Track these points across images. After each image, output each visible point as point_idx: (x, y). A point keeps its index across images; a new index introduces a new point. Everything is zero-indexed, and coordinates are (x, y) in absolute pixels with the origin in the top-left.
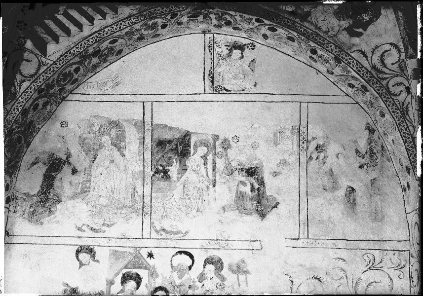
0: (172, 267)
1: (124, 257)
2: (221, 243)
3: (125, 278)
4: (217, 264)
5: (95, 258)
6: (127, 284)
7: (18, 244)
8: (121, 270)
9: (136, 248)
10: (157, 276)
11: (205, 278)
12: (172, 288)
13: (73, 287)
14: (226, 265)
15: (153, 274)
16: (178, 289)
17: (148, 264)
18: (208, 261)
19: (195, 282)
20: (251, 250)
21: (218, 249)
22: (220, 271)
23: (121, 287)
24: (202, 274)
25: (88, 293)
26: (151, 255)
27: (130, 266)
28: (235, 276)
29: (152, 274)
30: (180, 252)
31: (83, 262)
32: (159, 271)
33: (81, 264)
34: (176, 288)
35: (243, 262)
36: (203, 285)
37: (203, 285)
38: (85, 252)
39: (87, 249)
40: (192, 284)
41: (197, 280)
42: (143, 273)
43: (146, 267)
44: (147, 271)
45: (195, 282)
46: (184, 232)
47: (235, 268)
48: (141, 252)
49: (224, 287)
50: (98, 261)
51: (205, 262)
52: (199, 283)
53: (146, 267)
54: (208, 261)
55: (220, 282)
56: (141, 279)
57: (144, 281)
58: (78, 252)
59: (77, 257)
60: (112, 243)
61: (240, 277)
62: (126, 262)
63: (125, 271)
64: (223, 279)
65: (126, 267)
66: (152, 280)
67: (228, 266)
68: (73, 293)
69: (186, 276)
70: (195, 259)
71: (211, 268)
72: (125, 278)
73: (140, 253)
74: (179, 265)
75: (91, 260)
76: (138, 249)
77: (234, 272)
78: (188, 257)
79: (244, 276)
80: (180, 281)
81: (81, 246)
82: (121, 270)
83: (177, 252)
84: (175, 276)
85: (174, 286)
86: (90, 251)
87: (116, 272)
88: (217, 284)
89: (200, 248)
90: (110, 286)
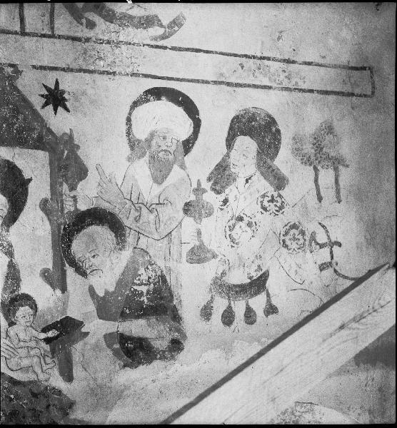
0: (133, 144)
2: (272, 70)
10: (82, 173)
11: (231, 179)
12: (134, 214)
15: (68, 165)
16: (152, 217)
19: (204, 191)
22: (273, 158)
29: (66, 167)
30: (157, 93)
32: (90, 155)
34: (144, 211)
36: (225, 201)
37: (225, 201)
40: (193, 198)
41: (207, 185)
42: (34, 165)
44: (42, 156)
45: (204, 191)
46: (165, 22)
47: (309, 149)
49: (281, 208)
51: (231, 128)
53: (40, 138)
55: (271, 190)
56: (24, 183)
57: (39, 190)
61: (322, 173)
66: (65, 187)
69: (176, 173)
70: (202, 116)
71: (246, 144)
73: (16, 89)
74: (152, 135)
77: (307, 161)
78: (179, 111)
80: (157, 189)
85: (138, 205)
88: (264, 196)
89: (215, 82)
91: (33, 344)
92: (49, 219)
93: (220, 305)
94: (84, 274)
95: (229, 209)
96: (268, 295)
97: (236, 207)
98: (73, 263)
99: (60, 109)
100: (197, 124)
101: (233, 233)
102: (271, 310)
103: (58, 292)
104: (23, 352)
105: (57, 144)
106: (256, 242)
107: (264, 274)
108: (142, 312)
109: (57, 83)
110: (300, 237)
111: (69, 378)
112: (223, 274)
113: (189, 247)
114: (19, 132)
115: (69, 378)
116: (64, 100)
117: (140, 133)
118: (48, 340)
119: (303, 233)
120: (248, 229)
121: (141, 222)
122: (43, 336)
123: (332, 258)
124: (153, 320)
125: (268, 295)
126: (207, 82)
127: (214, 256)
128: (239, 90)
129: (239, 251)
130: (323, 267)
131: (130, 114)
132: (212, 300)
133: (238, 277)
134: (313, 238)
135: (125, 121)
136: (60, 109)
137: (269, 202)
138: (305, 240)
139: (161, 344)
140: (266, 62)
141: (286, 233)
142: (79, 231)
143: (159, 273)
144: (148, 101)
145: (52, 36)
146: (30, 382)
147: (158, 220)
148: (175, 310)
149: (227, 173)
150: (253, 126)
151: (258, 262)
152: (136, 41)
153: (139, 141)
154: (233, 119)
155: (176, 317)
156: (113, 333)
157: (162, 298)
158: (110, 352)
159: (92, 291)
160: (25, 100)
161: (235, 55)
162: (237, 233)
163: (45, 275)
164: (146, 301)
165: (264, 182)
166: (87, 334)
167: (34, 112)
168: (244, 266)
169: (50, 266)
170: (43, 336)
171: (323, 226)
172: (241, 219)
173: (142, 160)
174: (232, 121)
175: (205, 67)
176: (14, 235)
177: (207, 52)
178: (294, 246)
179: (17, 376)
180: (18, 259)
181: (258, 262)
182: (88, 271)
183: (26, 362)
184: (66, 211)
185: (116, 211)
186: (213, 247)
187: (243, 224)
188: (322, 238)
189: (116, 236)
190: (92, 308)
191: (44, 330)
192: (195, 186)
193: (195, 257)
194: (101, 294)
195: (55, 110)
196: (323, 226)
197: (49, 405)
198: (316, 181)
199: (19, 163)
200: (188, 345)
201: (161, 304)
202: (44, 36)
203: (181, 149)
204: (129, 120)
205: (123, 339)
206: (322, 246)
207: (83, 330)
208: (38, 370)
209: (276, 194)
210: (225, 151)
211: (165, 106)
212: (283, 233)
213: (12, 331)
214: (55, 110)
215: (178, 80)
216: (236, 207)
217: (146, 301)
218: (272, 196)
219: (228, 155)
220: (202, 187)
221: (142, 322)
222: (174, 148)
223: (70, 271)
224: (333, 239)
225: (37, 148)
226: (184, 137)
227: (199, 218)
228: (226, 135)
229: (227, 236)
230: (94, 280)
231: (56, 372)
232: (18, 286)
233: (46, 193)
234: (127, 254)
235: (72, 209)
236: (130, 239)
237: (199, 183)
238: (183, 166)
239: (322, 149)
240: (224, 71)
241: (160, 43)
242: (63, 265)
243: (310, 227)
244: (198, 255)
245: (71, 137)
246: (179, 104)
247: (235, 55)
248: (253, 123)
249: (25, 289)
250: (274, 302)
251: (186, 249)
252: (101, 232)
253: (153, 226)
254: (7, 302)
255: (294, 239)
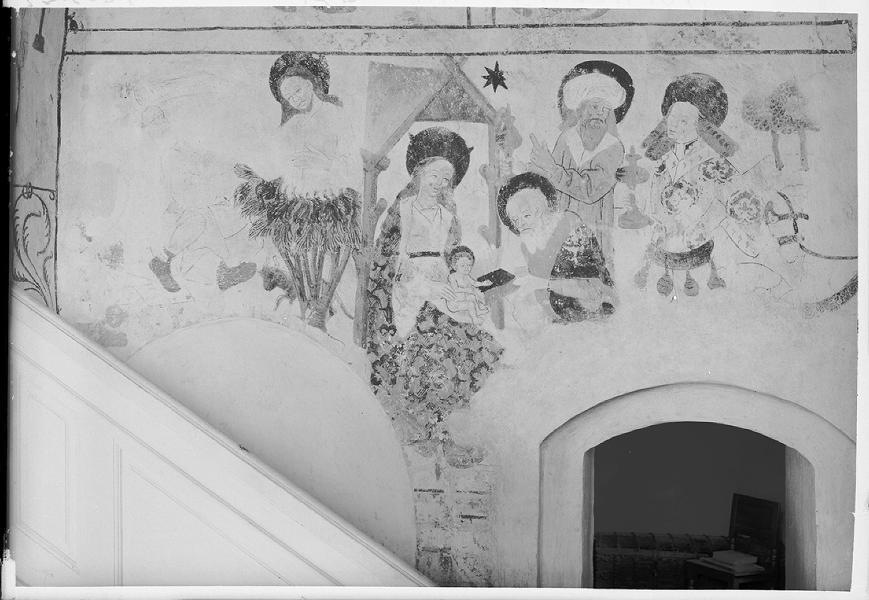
0: (564, 113)
1: (415, 84)
2: (718, 35)
3: (421, 150)
4: (711, 101)
5: (326, 91)
6: (427, 168)
7: (104, 53)
8: (406, 126)
9: (450, 56)
10: (518, 142)
12: (566, 178)
13: (267, 180)
14: (734, 103)
16: (584, 181)
17: (491, 107)
18: (677, 93)
20: (818, 52)
21: (709, 52)
22: (717, 124)
23: (408, 178)
24: (658, 134)
25: (312, 197)
26: (496, 78)
27: (433, 112)
28: (766, 137)
29: (502, 137)
31: (293, 104)
32: (524, 125)
33: (288, 111)
34: (576, 176)
35: (793, 90)
36: (662, 168)
37: (662, 168)
38: (298, 74)
39: (302, 63)
40: (626, 164)
41: (641, 152)
42: (474, 134)
43: (481, 114)
44: (483, 127)
47: (765, 112)
48: (465, 68)
50: (335, 100)
52: (648, 160)
53: (481, 114)
54: (677, 93)
55: (716, 157)
57: (478, 159)
58: (276, 74)
59: (275, 88)
60: (378, 44)
61: (783, 138)
62: (420, 102)
63: (417, 128)
64: (726, 147)
65: (421, 117)
66: (502, 155)
67: (741, 105)
68: (268, 198)
69: (608, 141)
70: (635, 85)
71: (685, 110)
72: (421, 150)
74: (583, 106)
75: (316, 98)
76: (457, 58)
78: (612, 81)
79: (795, 137)
81: (286, 56)
82: (406, 126)
83: (578, 67)
84: (574, 139)
85: (570, 170)
86: (313, 69)
87: (391, 131)
88: (707, 162)
89: (651, 52)
90: (376, 176)
91: (470, 291)
92: (488, 183)
93: (657, 271)
94: (517, 232)
95: (666, 176)
96: (713, 268)
97: (675, 172)
98: (508, 222)
99: (499, 87)
100: (630, 93)
101: (670, 200)
102: (717, 283)
103: (493, 247)
104: (460, 297)
105: (495, 116)
106: (697, 210)
107: (708, 243)
108: (574, 272)
109: (497, 65)
110: (753, 206)
111: (501, 326)
112: (660, 240)
113: (623, 212)
114: (464, 108)
115: (501, 326)
116: (503, 79)
117: (572, 102)
118: (483, 289)
119: (757, 203)
120: (688, 196)
121: (572, 186)
122: (479, 284)
123: (797, 231)
124: (583, 280)
125: (713, 268)
126: (641, 52)
127: (650, 223)
128: (678, 57)
129: (678, 218)
130: (782, 242)
131: (562, 87)
132: (647, 267)
133: (677, 245)
134: (770, 208)
135: (557, 93)
136: (499, 87)
137: (714, 168)
138: (759, 210)
139: (590, 304)
140: (711, 27)
141: (735, 202)
142: (513, 192)
143: (590, 236)
144: (580, 74)
145: (494, 26)
146: (466, 324)
147: (589, 185)
148: (606, 273)
149: (664, 139)
150: (693, 92)
151: (701, 231)
152: (568, 22)
153: (571, 111)
154: (671, 84)
155: (607, 281)
156: (541, 290)
157: (592, 260)
158: (540, 308)
159: (524, 248)
160: (468, 81)
161: (675, 25)
162: (675, 199)
163: (483, 232)
164: (576, 261)
165: (707, 147)
166: (517, 287)
167: (478, 92)
168: (683, 234)
169: (487, 224)
170: (479, 284)
171: (783, 196)
172: (680, 186)
173: (573, 129)
174: (669, 88)
175: (641, 39)
176: (458, 194)
177: (642, 24)
178: (745, 215)
179: (456, 317)
180: (459, 215)
181: (701, 231)
182: (520, 230)
183: (462, 306)
184: (502, 175)
185: (547, 176)
186: (648, 212)
187: (682, 191)
188: (781, 208)
189: (548, 199)
190: (522, 262)
191: (480, 280)
192: (628, 151)
193: (627, 223)
194: (532, 251)
195: (495, 88)
196: (783, 196)
197: (481, 349)
198: (775, 147)
199: (463, 135)
200: (621, 311)
201: (589, 265)
202: (486, 27)
203: (613, 117)
204: (561, 93)
205: (553, 296)
206: (781, 218)
207: (515, 282)
208: (472, 313)
209: (722, 161)
210: (661, 117)
211: (597, 77)
212: (731, 201)
213: (453, 277)
214: (495, 88)
215: (611, 53)
216: (675, 172)
217: (576, 261)
218: (718, 163)
219: (664, 122)
220: (637, 153)
221: (573, 281)
222: (605, 116)
223: (505, 228)
224: (797, 211)
225: (478, 121)
226: (617, 105)
227: (632, 185)
228: (662, 102)
229: (664, 202)
230: (525, 237)
231: (488, 318)
232: (459, 239)
233: (485, 160)
234: (559, 215)
235: (508, 173)
236: (561, 200)
237: (632, 148)
238: (615, 135)
239: (782, 113)
240: (661, 40)
241: (592, 22)
242: (498, 223)
243: (764, 197)
244: (633, 220)
245: (507, 111)
246: (612, 75)
247: (675, 25)
248: (694, 89)
249: (463, 243)
250: (721, 274)
251: (618, 214)
252: (531, 196)
253: (584, 190)
254: (449, 253)
255: (745, 208)
